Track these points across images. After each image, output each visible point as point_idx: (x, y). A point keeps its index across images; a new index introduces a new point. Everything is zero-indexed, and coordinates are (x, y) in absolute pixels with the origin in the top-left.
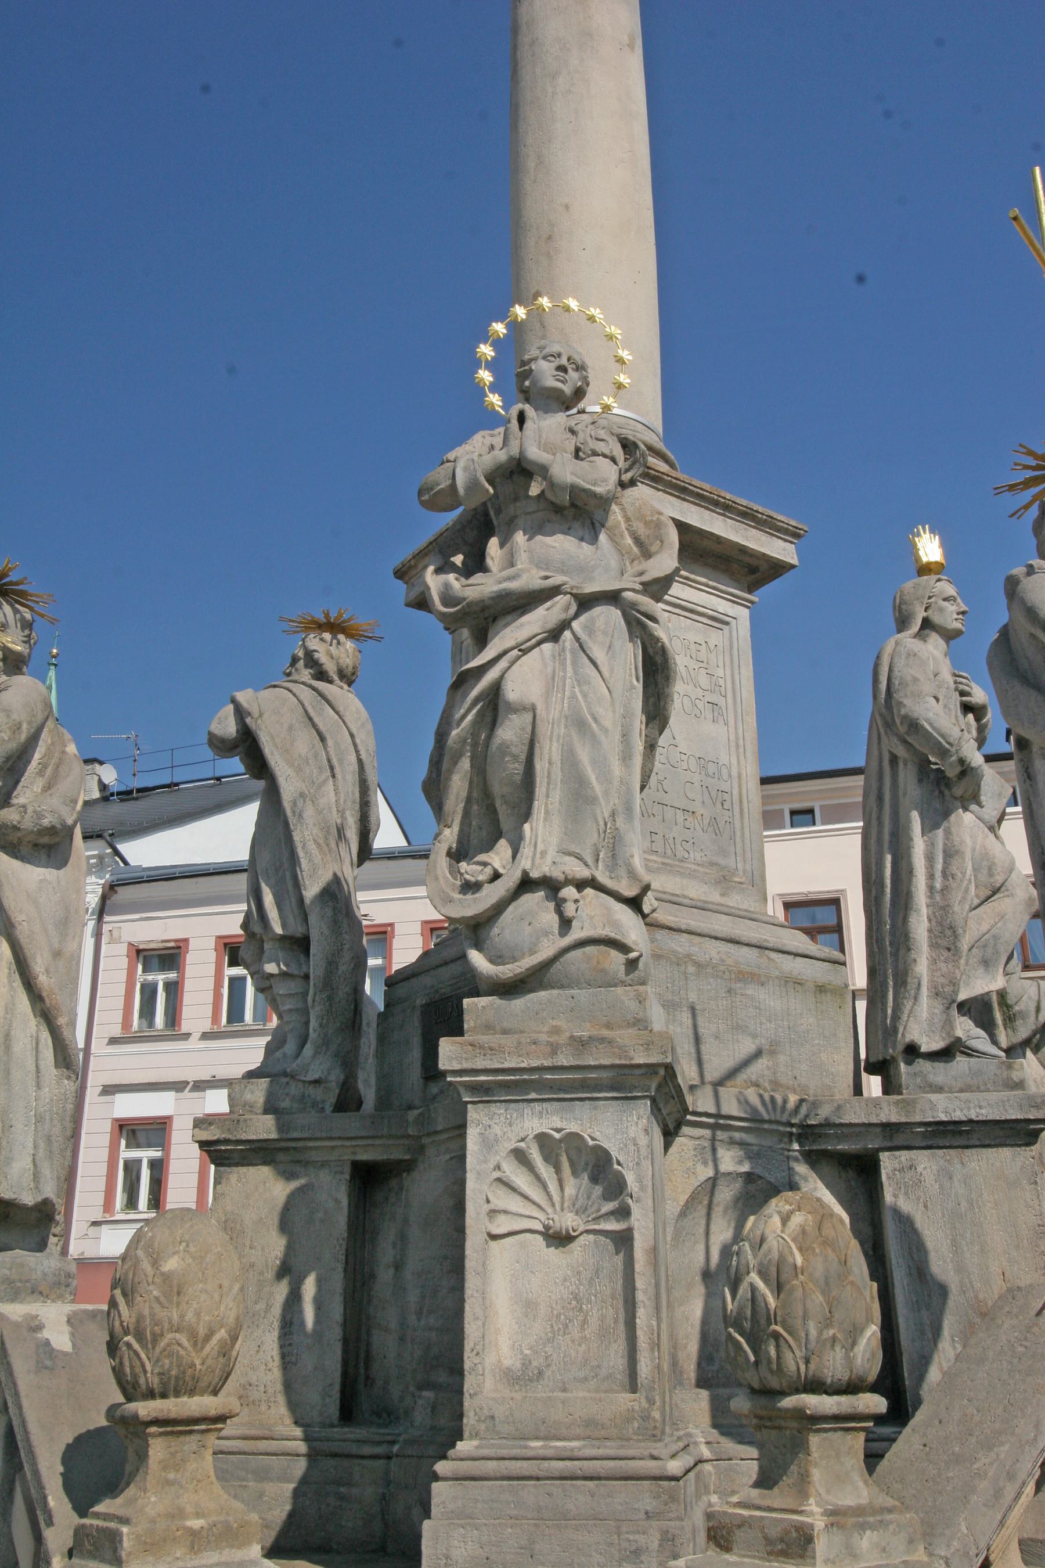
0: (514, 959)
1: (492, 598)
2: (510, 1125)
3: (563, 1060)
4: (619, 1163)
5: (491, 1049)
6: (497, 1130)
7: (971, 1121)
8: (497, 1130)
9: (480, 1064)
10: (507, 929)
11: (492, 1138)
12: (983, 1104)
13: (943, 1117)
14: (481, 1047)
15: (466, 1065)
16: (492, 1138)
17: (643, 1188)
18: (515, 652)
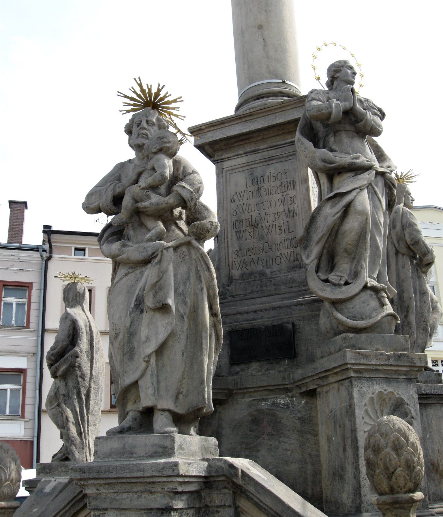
0: (362, 319)
1: (348, 165)
2: (369, 387)
3: (391, 362)
4: (408, 404)
5: (366, 356)
6: (364, 389)
7: (432, 394)
8: (364, 389)
9: (363, 361)
10: (356, 305)
11: (363, 392)
12: (436, 388)
13: (424, 392)
14: (362, 355)
15: (357, 362)
16: (363, 392)
17: (417, 414)
18: (358, 190)
